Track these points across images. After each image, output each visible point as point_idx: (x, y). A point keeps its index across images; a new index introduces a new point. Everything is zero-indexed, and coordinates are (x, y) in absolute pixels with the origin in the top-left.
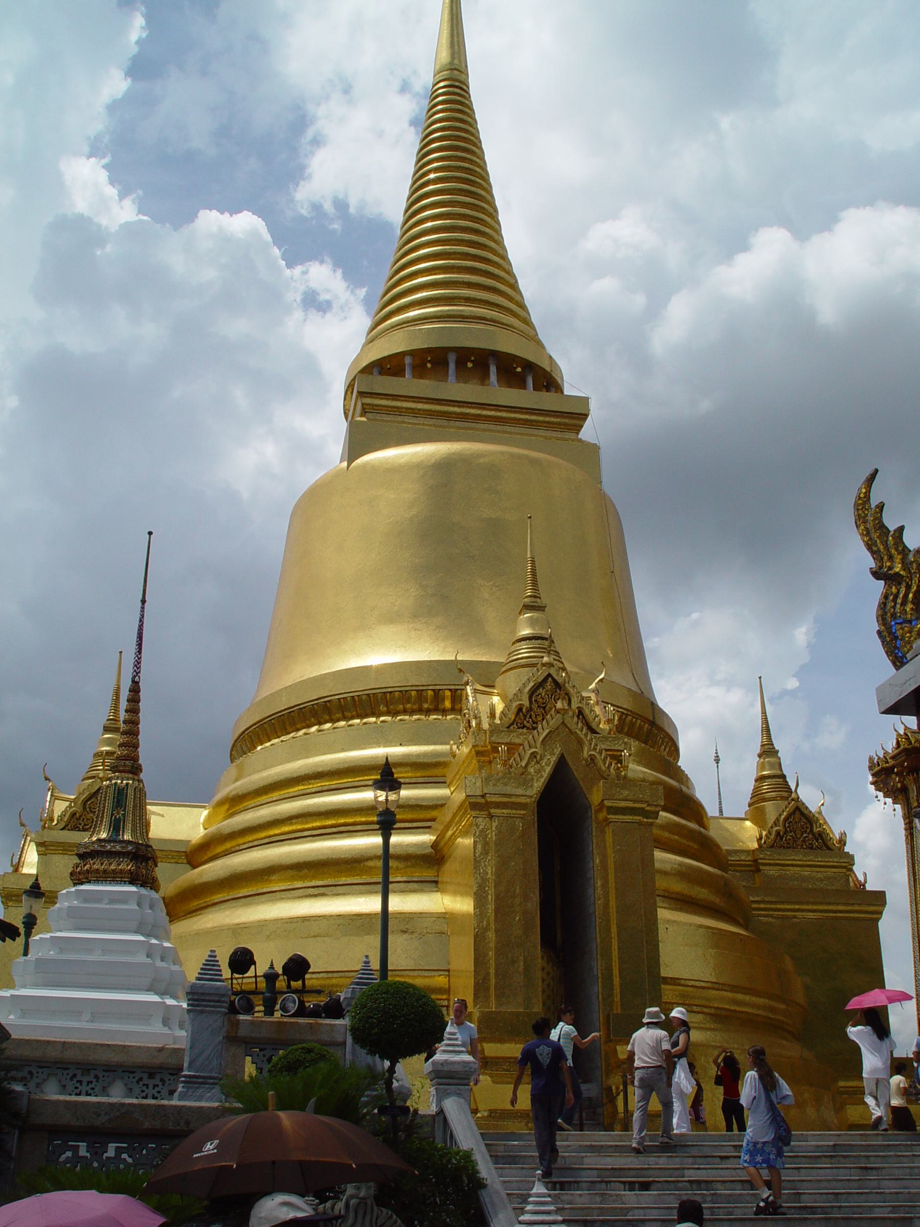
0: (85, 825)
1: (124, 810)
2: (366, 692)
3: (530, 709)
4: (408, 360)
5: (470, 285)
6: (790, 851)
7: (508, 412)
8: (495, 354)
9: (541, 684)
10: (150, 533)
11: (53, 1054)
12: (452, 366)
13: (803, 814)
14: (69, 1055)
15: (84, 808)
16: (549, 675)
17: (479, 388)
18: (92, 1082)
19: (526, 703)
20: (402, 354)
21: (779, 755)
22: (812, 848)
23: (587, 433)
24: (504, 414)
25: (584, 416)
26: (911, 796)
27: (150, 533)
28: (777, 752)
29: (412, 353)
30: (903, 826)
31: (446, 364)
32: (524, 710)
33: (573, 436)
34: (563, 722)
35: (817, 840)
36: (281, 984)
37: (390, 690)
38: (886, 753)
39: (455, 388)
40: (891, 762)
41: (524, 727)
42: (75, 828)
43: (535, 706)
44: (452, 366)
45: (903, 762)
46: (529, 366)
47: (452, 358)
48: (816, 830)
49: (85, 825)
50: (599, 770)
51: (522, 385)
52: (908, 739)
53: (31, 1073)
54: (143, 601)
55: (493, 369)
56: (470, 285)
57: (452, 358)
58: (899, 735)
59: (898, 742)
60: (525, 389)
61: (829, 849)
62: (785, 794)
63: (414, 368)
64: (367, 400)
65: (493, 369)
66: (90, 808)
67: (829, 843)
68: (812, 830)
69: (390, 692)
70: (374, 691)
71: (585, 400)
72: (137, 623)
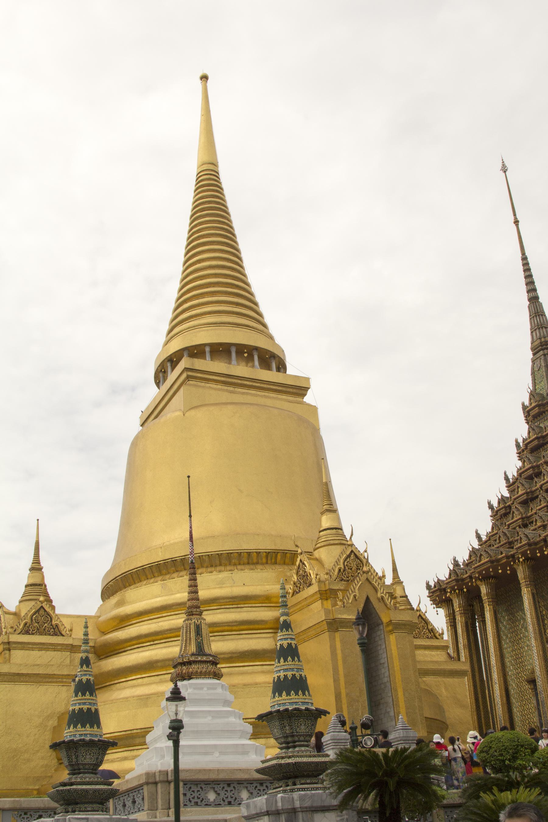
0: (33, 631)
1: (202, 637)
2: (217, 553)
3: (344, 571)
4: (207, 349)
5: (237, 304)
6: (418, 640)
7: (268, 384)
8: (256, 349)
9: (349, 556)
10: (189, 477)
11: (213, 776)
12: (234, 355)
13: (422, 618)
14: (221, 776)
15: (32, 620)
16: (352, 551)
17: (251, 369)
18: (199, 791)
19: (342, 566)
20: (205, 345)
21: (404, 584)
22: (428, 638)
23: (308, 399)
24: (265, 386)
25: (307, 389)
26: (455, 605)
27: (189, 477)
28: (402, 582)
29: (211, 345)
30: (445, 621)
31: (229, 353)
32: (342, 570)
33: (299, 399)
34: (367, 579)
35: (430, 633)
36: (359, 732)
37: (231, 552)
38: (438, 580)
39: (240, 369)
40: (444, 587)
41: (342, 580)
42: (27, 633)
43: (347, 568)
44: (234, 355)
45: (455, 586)
46: (273, 356)
47: (233, 350)
48: (430, 627)
49: (33, 631)
50: (386, 605)
51: (269, 368)
52: (456, 573)
53: (201, 788)
54: (190, 516)
55: (256, 358)
56: (237, 304)
57: (233, 350)
58: (450, 570)
59: (450, 574)
60: (271, 370)
61: (437, 638)
62: (409, 607)
63: (211, 352)
64: (190, 373)
65: (256, 358)
66: (35, 620)
67: (437, 635)
68: (427, 628)
69: (231, 553)
70: (221, 552)
71: (307, 379)
72: (188, 529)
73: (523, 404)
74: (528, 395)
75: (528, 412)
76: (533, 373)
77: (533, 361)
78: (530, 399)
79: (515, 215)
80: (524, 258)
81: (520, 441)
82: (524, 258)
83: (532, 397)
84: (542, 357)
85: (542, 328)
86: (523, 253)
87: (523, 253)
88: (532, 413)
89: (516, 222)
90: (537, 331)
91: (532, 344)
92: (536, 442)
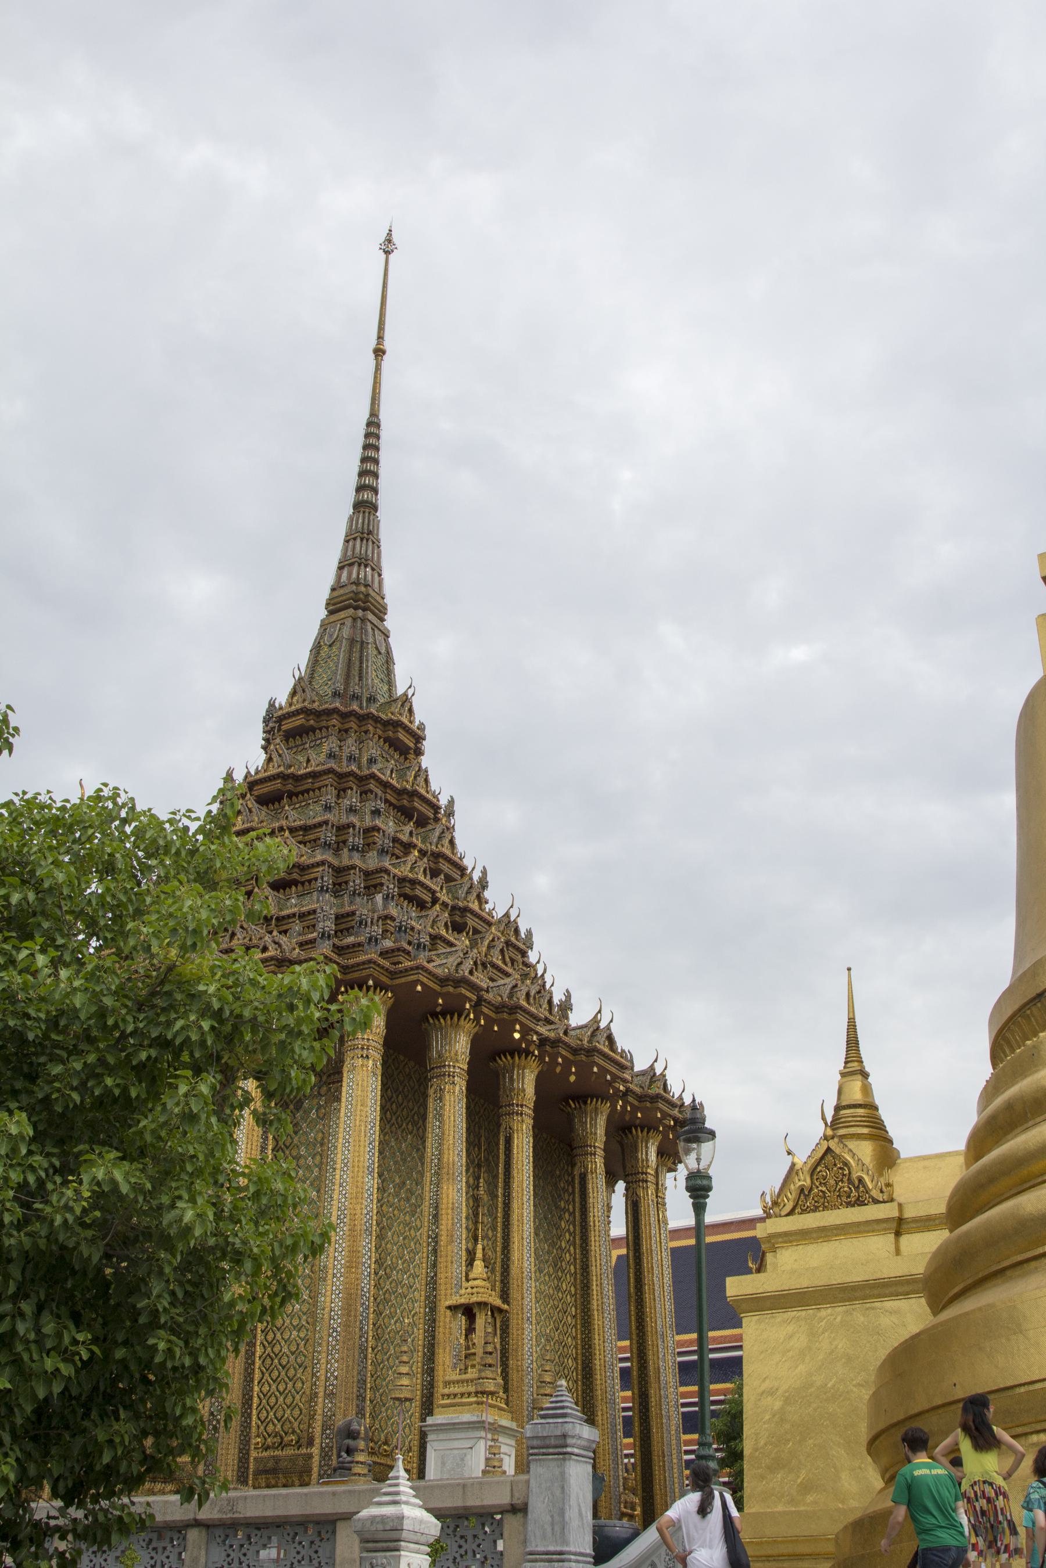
73: (272, 704)
74: (291, 684)
75: (280, 719)
76: (317, 649)
77: (324, 626)
78: (294, 693)
79: (380, 338)
80: (373, 424)
81: (239, 777)
82: (373, 424)
83: (299, 689)
84: (349, 622)
85: (366, 566)
86: (374, 413)
87: (374, 413)
88: (287, 726)
89: (379, 352)
90: (355, 568)
91: (333, 590)
92: (277, 785)
